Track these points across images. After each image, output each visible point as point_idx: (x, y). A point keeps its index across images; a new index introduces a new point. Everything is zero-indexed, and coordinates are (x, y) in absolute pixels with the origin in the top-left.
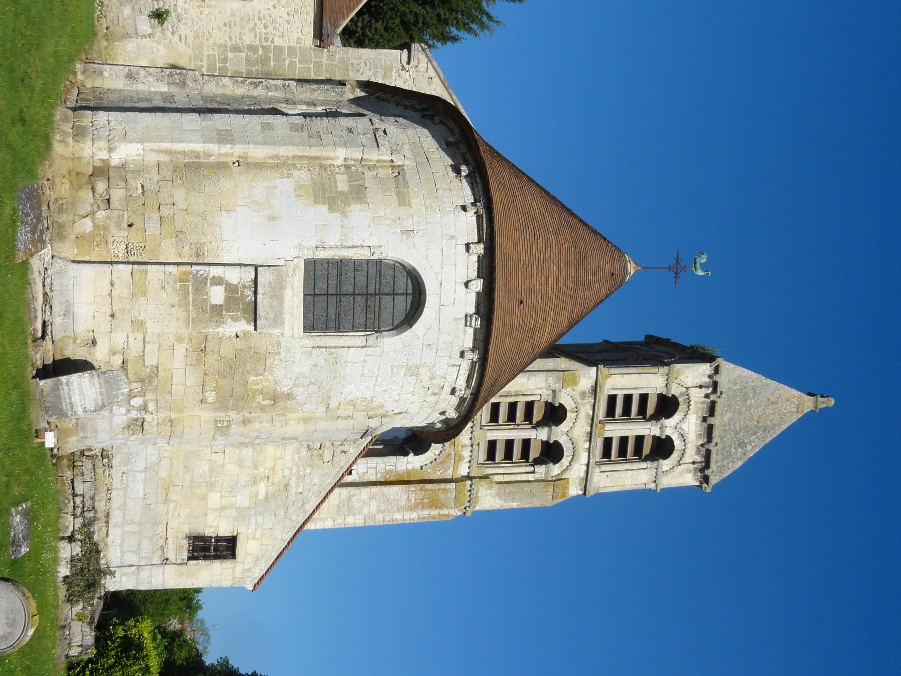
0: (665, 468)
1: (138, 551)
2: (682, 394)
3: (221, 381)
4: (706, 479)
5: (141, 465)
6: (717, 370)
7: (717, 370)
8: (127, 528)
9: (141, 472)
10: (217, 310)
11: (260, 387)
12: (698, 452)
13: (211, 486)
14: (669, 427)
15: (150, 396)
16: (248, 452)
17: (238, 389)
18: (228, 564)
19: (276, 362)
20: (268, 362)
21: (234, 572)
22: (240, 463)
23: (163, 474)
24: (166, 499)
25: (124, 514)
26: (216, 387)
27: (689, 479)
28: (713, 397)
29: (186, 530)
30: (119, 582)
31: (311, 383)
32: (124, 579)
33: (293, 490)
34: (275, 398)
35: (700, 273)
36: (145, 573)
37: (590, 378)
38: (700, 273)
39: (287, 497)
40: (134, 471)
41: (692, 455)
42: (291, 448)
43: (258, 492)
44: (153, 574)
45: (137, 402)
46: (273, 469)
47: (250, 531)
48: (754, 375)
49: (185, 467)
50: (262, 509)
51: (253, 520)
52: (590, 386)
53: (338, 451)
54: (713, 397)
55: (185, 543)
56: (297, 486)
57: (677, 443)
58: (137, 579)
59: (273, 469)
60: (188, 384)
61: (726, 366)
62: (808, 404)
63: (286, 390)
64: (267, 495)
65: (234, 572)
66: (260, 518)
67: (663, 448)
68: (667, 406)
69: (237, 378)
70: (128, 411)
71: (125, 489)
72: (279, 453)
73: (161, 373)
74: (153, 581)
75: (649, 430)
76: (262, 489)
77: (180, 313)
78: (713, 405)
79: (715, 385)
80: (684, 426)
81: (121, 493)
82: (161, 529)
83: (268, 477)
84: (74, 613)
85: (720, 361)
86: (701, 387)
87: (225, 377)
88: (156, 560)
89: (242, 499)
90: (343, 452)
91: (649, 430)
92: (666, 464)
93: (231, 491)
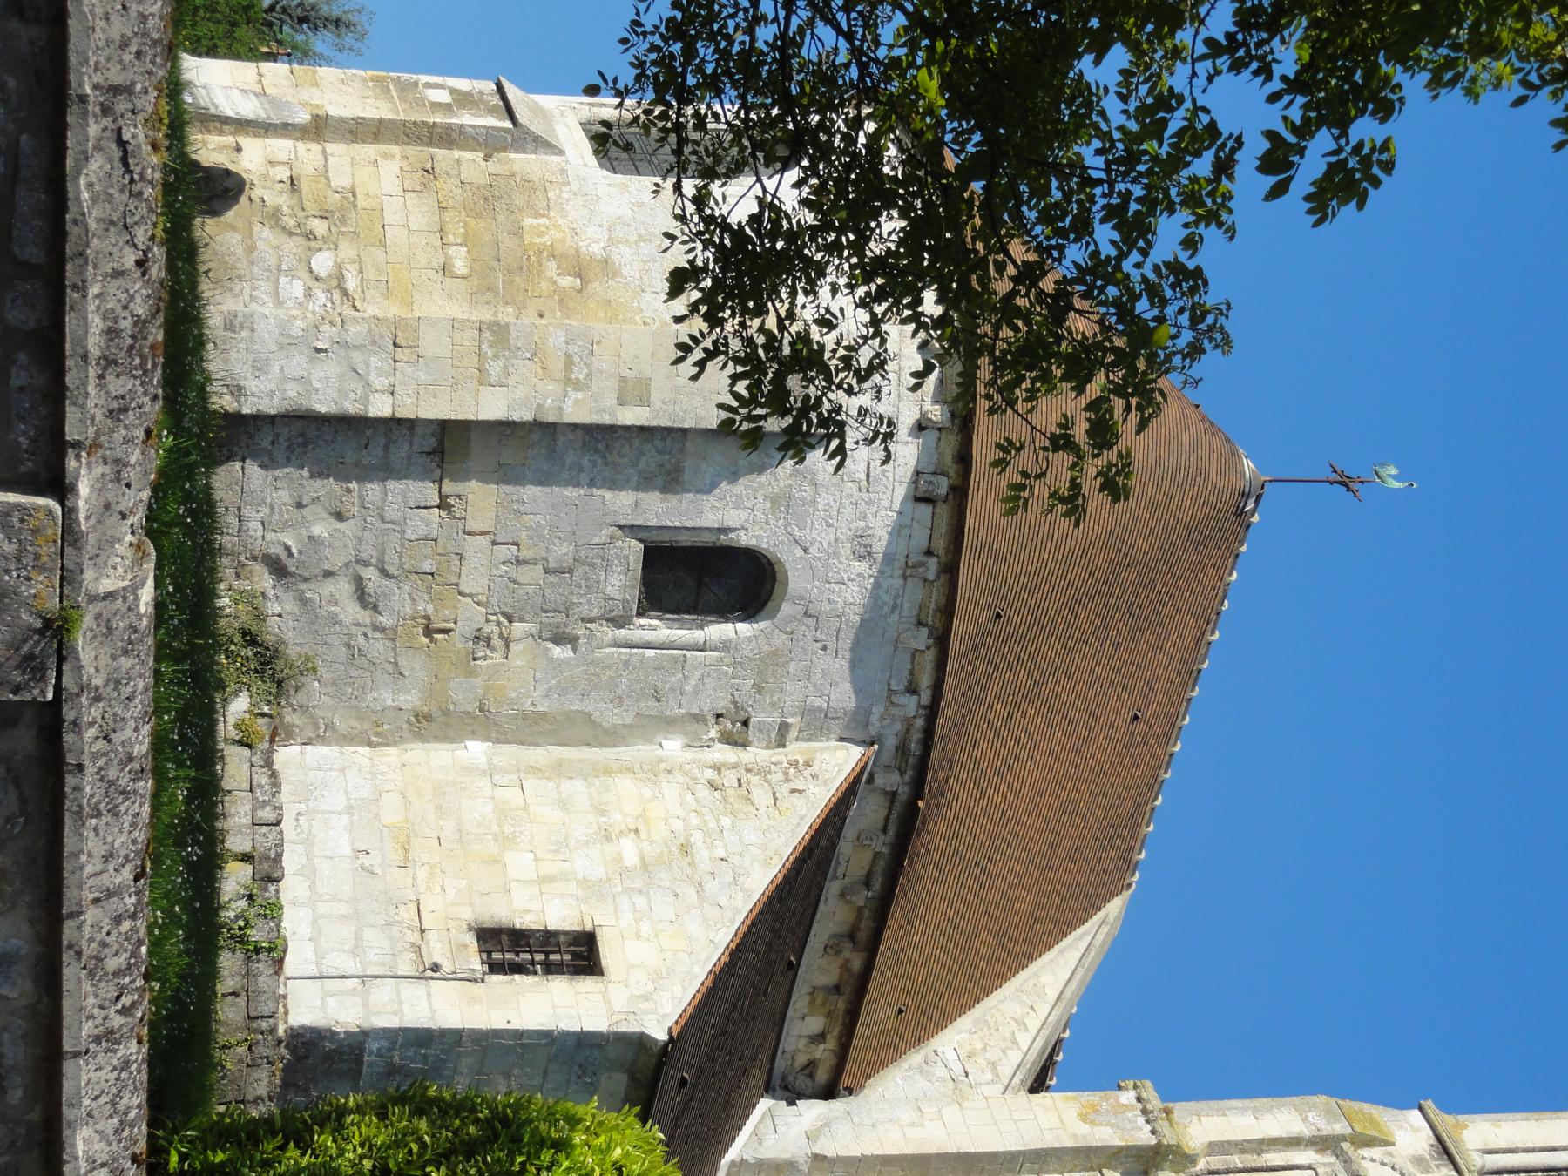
1: (356, 950)
3: (472, 223)
5: (339, 802)
8: (322, 908)
9: (339, 813)
11: (546, 240)
13: (506, 841)
15: (347, 250)
16: (576, 789)
17: (507, 242)
18: (587, 983)
19: (566, 195)
20: (551, 195)
21: (607, 1001)
22: (563, 804)
23: (390, 817)
24: (407, 859)
25: (313, 882)
26: (466, 235)
29: (467, 914)
31: (641, 238)
32: (331, 1001)
33: (703, 855)
34: (581, 268)
35: (1396, 485)
36: (383, 992)
37: (1416, 1130)
38: (1396, 485)
39: (692, 864)
40: (323, 812)
42: (671, 790)
43: (619, 854)
44: (404, 996)
45: (323, 262)
46: (643, 816)
47: (623, 923)
49: (439, 807)
50: (639, 884)
51: (624, 903)
52: (1427, 1148)
53: (783, 790)
56: (711, 847)
58: (366, 1005)
59: (643, 816)
60: (414, 227)
63: (597, 249)
64: (643, 860)
65: (607, 1001)
66: (640, 901)
69: (501, 218)
70: (308, 292)
71: (308, 842)
72: (647, 792)
73: (361, 202)
74: (406, 1010)
76: (629, 850)
81: (301, 849)
82: (407, 914)
83: (636, 831)
84: (231, 720)
87: (478, 215)
88: (406, 966)
89: (589, 863)
90: (793, 791)
93: (557, 851)
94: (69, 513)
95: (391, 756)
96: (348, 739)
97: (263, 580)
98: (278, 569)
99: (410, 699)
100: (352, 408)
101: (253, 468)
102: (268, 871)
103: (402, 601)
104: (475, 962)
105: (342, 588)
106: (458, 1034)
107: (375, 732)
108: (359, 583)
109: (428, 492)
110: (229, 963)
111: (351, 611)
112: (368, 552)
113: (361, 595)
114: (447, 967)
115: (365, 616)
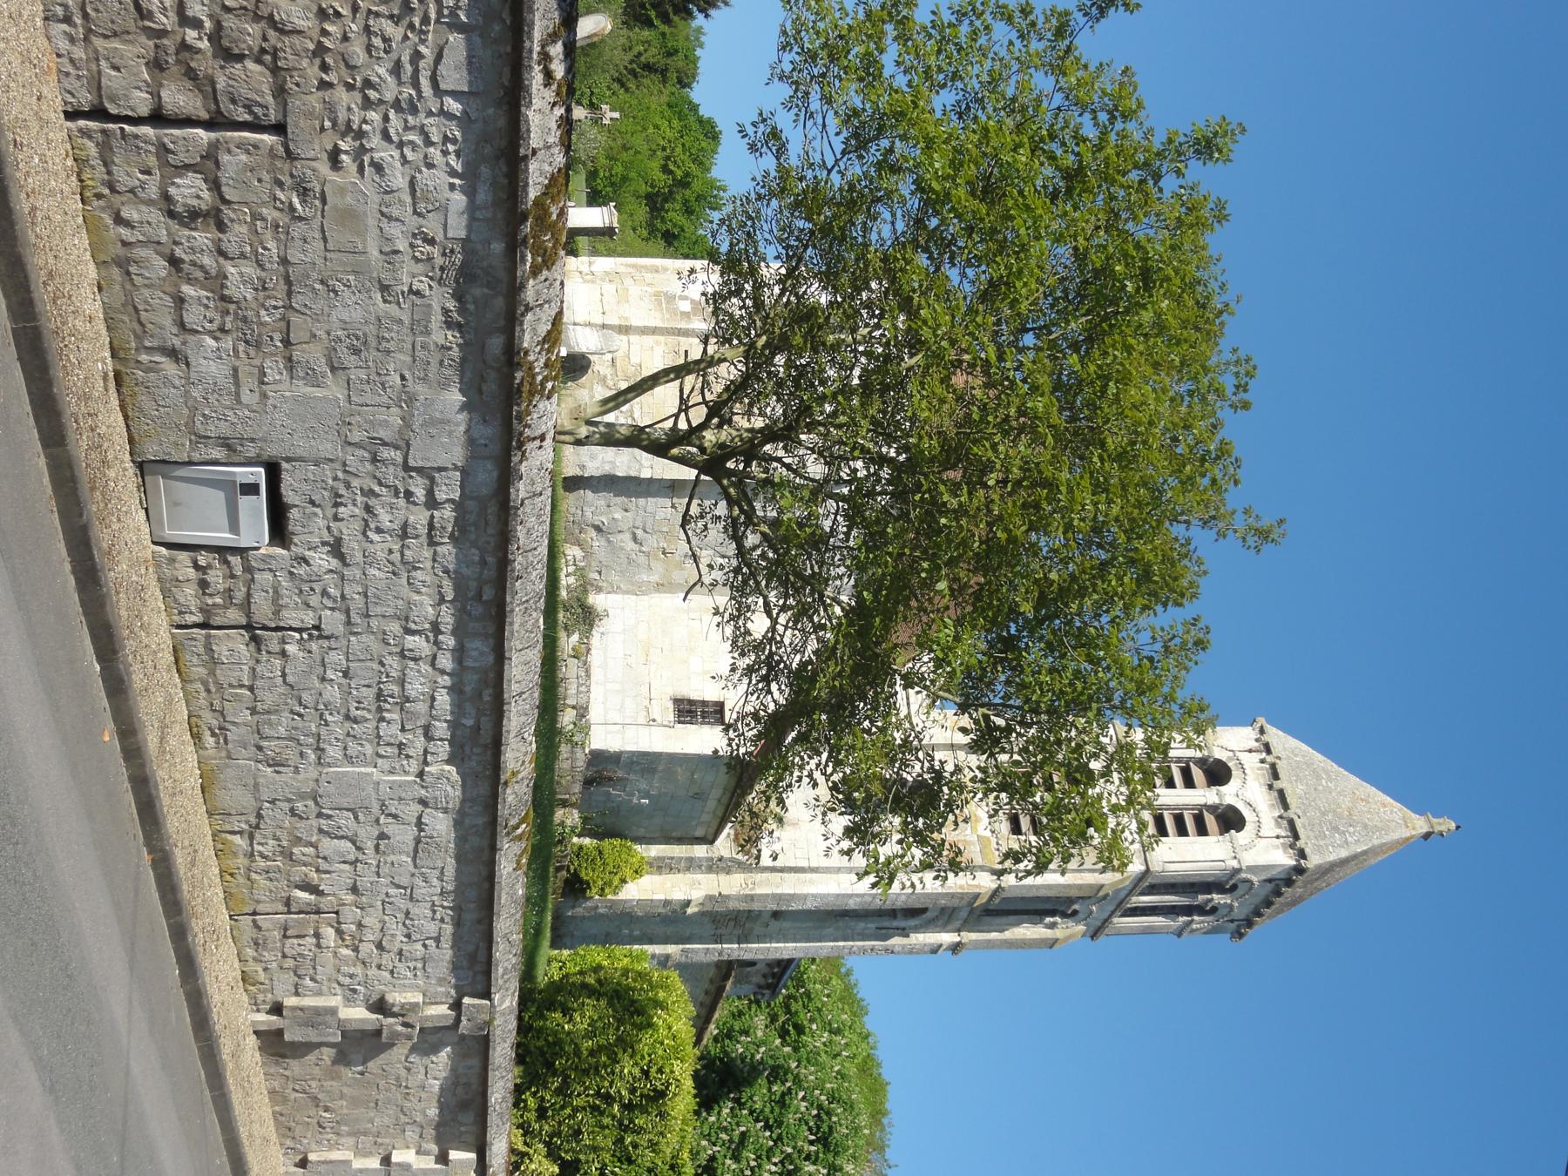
0: (1242, 842)
2: (1230, 759)
4: (1302, 854)
6: (1262, 731)
7: (1262, 731)
10: (685, 315)
12: (1279, 825)
14: (1228, 794)
27: (1283, 859)
28: (1270, 759)
30: (602, 739)
36: (631, 732)
41: (1270, 828)
48: (1320, 757)
54: (1270, 759)
55: (671, 705)
57: (1246, 812)
61: (1270, 729)
62: (1420, 825)
67: (1230, 820)
68: (1218, 774)
75: (1204, 795)
77: (658, 315)
78: (1273, 766)
79: (1267, 748)
80: (1249, 796)
82: (645, 690)
85: (1261, 721)
86: (1250, 751)
88: (642, 720)
91: (1204, 795)
92: (1241, 837)
94: (492, 1005)
95: (645, 600)
96: (627, 592)
97: (593, 533)
98: (598, 529)
99: (655, 578)
100: (633, 474)
101: (588, 493)
102: (582, 711)
103: (652, 542)
104: (671, 716)
105: (627, 536)
106: (660, 754)
107: (638, 590)
108: (634, 535)
109: (668, 502)
110: (564, 749)
111: (630, 545)
112: (639, 523)
113: (635, 539)
114: (659, 721)
115: (636, 547)
